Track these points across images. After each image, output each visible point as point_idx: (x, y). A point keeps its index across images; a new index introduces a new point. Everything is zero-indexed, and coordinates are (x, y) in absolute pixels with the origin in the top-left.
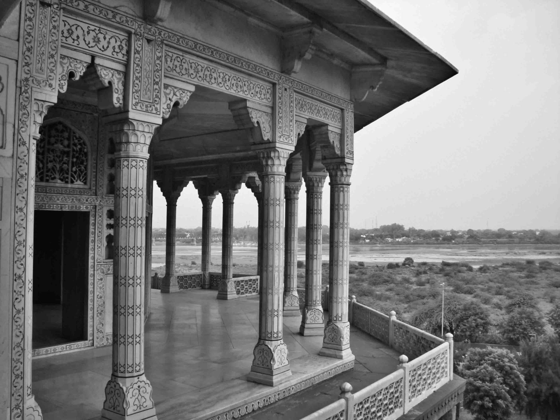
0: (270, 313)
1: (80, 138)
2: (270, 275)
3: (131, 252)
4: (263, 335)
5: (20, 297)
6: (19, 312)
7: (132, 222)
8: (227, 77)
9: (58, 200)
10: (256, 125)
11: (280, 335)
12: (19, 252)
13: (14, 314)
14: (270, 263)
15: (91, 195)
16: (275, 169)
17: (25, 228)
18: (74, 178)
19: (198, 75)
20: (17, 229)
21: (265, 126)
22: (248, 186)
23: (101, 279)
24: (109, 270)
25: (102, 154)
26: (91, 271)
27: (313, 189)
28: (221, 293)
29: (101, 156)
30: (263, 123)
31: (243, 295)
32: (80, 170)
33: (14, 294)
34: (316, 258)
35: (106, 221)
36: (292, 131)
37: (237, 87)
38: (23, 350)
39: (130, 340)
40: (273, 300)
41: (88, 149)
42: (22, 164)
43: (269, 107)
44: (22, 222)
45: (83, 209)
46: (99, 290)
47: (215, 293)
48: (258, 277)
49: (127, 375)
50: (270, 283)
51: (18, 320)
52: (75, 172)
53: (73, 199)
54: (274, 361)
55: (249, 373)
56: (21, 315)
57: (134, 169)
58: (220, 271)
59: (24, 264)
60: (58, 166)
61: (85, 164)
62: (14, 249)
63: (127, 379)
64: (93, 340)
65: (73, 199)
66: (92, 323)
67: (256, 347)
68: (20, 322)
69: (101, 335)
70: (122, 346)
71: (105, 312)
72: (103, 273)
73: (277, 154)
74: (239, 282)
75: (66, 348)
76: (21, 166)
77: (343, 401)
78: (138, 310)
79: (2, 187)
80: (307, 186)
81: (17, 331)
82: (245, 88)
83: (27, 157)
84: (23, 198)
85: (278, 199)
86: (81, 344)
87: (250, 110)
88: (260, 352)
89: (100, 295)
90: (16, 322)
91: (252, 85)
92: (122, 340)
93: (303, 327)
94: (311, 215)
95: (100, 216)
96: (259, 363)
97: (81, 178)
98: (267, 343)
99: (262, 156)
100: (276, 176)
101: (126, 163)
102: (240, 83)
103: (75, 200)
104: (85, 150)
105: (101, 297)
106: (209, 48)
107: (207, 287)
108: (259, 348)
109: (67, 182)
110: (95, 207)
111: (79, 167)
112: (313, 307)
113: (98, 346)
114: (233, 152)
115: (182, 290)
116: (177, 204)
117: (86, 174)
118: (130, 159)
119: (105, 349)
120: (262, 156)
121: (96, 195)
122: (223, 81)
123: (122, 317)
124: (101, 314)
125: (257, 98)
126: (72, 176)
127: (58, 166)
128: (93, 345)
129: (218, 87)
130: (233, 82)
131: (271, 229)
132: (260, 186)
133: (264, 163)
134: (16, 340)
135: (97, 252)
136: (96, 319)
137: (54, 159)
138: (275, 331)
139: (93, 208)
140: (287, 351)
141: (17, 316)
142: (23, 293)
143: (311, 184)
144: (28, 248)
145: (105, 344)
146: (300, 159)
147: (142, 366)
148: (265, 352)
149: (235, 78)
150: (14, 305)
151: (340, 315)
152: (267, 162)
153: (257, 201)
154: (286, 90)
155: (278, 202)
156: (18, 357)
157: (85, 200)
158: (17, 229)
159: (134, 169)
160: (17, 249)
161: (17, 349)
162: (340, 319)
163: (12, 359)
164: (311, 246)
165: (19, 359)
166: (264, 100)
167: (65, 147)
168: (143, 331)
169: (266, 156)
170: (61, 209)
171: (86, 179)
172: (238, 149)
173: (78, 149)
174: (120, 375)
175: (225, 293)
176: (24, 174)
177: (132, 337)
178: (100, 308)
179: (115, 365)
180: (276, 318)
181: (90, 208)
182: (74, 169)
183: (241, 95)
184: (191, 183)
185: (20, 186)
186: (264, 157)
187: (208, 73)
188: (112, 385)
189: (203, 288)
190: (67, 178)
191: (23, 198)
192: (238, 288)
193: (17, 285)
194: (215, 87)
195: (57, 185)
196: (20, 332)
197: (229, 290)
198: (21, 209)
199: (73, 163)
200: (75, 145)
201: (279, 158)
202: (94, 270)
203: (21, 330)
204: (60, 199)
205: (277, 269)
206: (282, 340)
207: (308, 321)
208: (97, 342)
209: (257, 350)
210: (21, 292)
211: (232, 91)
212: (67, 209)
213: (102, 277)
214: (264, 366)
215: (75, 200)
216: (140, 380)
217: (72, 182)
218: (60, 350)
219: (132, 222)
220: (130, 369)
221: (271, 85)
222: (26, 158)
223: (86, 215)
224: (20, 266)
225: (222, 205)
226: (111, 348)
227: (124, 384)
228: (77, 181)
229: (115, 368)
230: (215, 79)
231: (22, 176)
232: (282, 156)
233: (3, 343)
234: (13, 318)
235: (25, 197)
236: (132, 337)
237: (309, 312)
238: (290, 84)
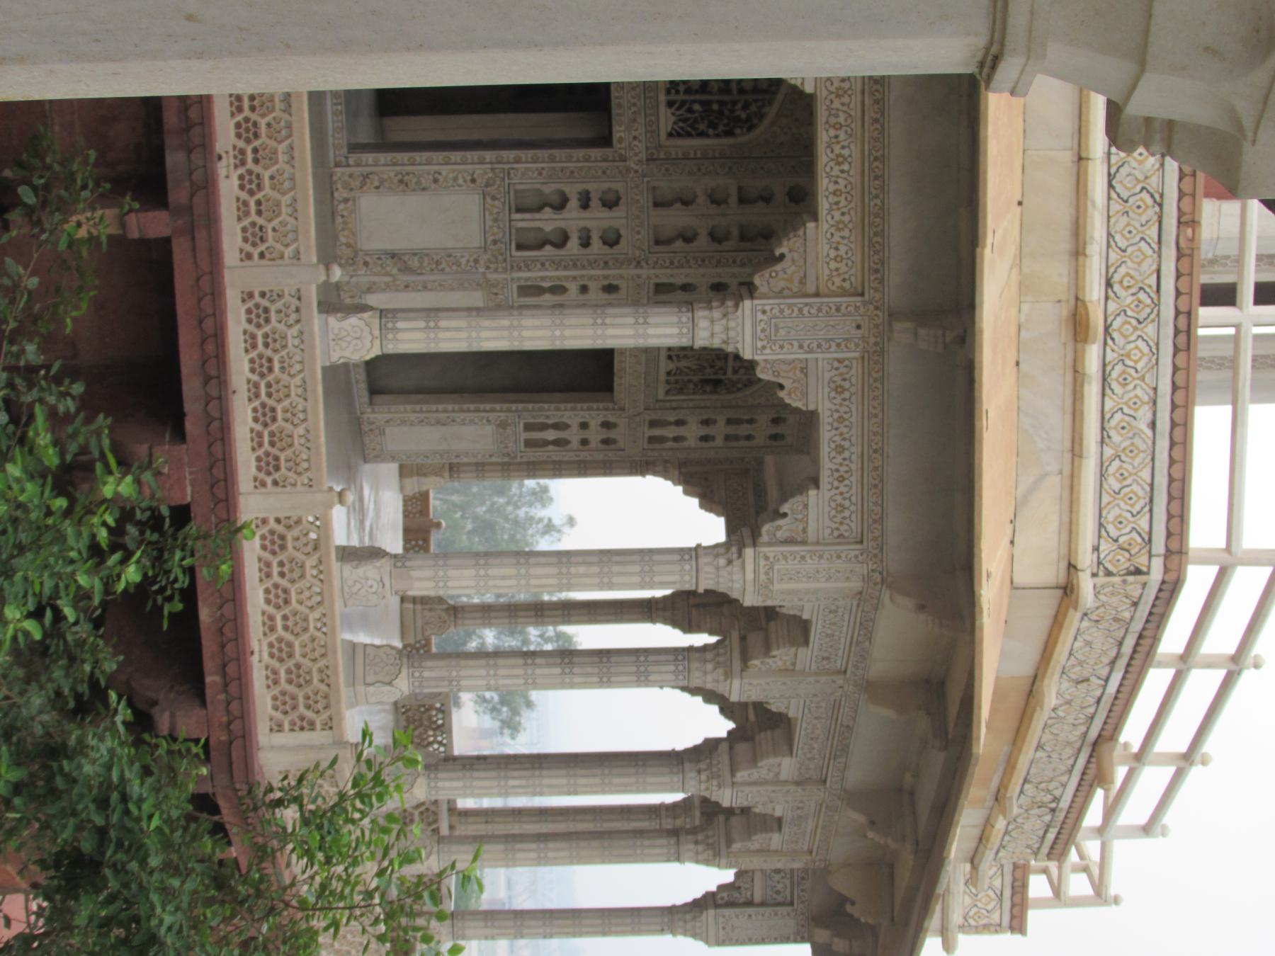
1: (761, 117)
8: (846, 167)
10: (777, 252)
15: (647, 148)
18: (678, 109)
19: (833, 96)
21: (781, 275)
23: (473, 181)
24: (494, 198)
29: (730, 168)
30: (784, 271)
32: (696, 120)
34: (526, 664)
36: (782, 347)
37: (834, 193)
41: (743, 138)
43: (818, 287)
45: (618, 131)
46: (451, 175)
52: (690, 111)
53: (634, 105)
61: (711, 131)
64: (348, 166)
69: (358, 184)
72: (487, 185)
73: (730, 310)
75: (336, 104)
77: (315, 260)
82: (837, 215)
87: (801, 233)
89: (441, 178)
91: (846, 233)
95: (604, 173)
97: (681, 124)
102: (842, 199)
103: (633, 109)
104: (738, 131)
105: (436, 181)
106: (883, 114)
110: (623, 159)
111: (703, 119)
112: (405, 660)
113: (335, 178)
117: (689, 135)
121: (648, 160)
122: (838, 156)
124: (401, 181)
125: (826, 247)
126: (683, 103)
128: (337, 165)
129: (824, 145)
130: (842, 182)
136: (389, 172)
145: (336, 195)
149: (849, 187)
151: (408, 564)
153: (689, 899)
154: (858, 327)
155: (641, 320)
162: (399, 564)
166: (827, 272)
171: (679, 135)
173: (738, 113)
178: (414, 180)
182: (697, 107)
183: (823, 205)
187: (842, 119)
190: (677, 92)
194: (823, 137)
199: (709, 103)
200: (746, 106)
201: (725, 315)
208: (343, 174)
211: (825, 181)
213: (478, 181)
215: (633, 109)
217: (670, 104)
221: (860, 290)
223: (604, 140)
230: (836, 137)
238: (872, 340)
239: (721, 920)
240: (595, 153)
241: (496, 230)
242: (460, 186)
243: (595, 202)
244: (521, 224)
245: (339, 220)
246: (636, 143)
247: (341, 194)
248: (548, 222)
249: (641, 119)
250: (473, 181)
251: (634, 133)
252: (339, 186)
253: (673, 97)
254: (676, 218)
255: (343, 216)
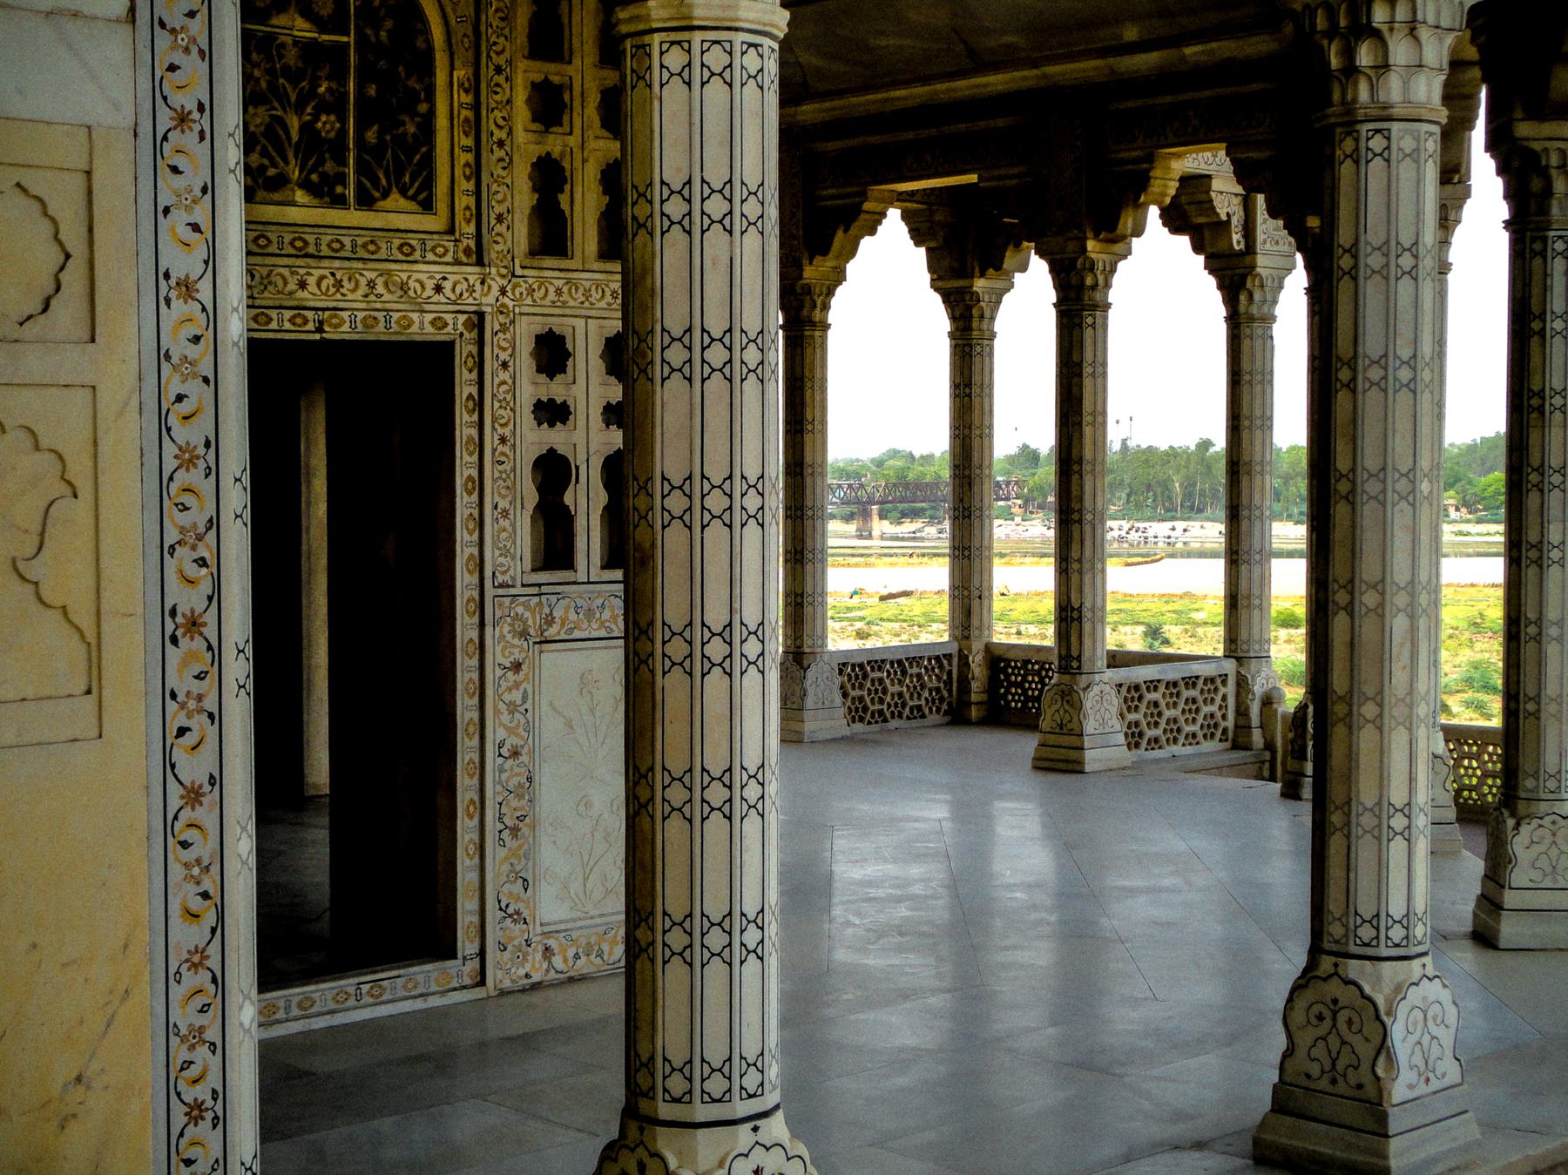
0: (1367, 820)
2: (1367, 629)
3: (716, 502)
4: (1336, 930)
5: (199, 723)
6: (194, 796)
7: (717, 355)
9: (303, 285)
11: (1419, 931)
12: (187, 499)
13: (174, 803)
14: (1368, 569)
15: (457, 262)
16: (1393, 89)
17: (212, 382)
20: (174, 387)
22: (1175, 220)
23: (517, 666)
24: (550, 620)
25: (501, 60)
26: (465, 628)
27: (1544, 211)
28: (1052, 739)
29: (499, 70)
31: (1157, 754)
33: (172, 706)
35: (530, 387)
38: (218, 981)
39: (716, 939)
40: (1382, 752)
42: (177, 58)
44: (193, 351)
45: (421, 328)
46: (505, 718)
47: (1025, 745)
48: (1230, 667)
49: (703, 1112)
50: (1366, 669)
51: (190, 835)
52: (378, 151)
53: (371, 284)
54: (1391, 1061)
55: (1263, 1125)
56: (205, 815)
57: (716, 88)
58: (1049, 642)
59: (212, 561)
60: (294, 123)
62: (164, 482)
63: (701, 1132)
64: (482, 954)
65: (371, 284)
66: (474, 876)
67: (1297, 988)
68: (204, 849)
70: (676, 969)
71: (533, 827)
72: (524, 634)
74: (1137, 688)
76: (172, 68)
78: (752, 792)
79: (89, 173)
80: (1513, 195)
81: (192, 889)
83: (201, 18)
84: (196, 228)
85: (1406, 241)
86: (426, 974)
88: (1320, 1018)
90: (185, 845)
92: (677, 939)
93: (1490, 903)
94: (1535, 341)
96: (1315, 1069)
98: (1353, 968)
99: (1321, 23)
100: (1396, 127)
101: (675, 59)
103: (380, 289)
105: (515, 754)
107: (974, 713)
108: (1309, 995)
109: (339, 202)
110: (478, 321)
112: (1543, 807)
113: (507, 984)
114: (1104, 53)
115: (859, 727)
116: (832, 317)
117: (428, 161)
118: (697, 37)
119: (536, 998)
120: (1321, 23)
121: (480, 262)
123: (675, 822)
124: (515, 831)
126: (362, 168)
127: (294, 123)
128: (482, 982)
131: (1371, 402)
132: (1237, 222)
133: (1335, 62)
134: (187, 936)
135: (492, 530)
137: (273, 86)
138: (1397, 908)
139: (469, 325)
140: (1452, 1012)
141: (186, 815)
142: (210, 704)
143: (1536, 184)
144: (227, 481)
145: (536, 978)
146: (1471, 64)
147: (773, 1071)
148: (1343, 1016)
150: (170, 766)
152: (1349, 54)
153: (1218, 296)
155: (1406, 261)
156: (200, 1020)
157: (430, 284)
158: (174, 387)
159: (716, 88)
160: (174, 487)
161: (191, 980)
163: (170, 1028)
164: (1533, 500)
165: (202, 1029)
167: (323, 29)
168: (773, 896)
169: (1343, 23)
170: (320, 330)
171: (429, 184)
172: (1131, 34)
174: (665, 1111)
175: (1073, 740)
176: (191, 105)
177: (725, 923)
178: (514, 803)
179: (640, 1067)
180: (1397, 847)
181: (456, 325)
182: (371, 136)
184: (894, 214)
185: (175, 170)
186: (1333, 32)
188: (629, 1162)
189: (957, 717)
191: (196, 228)
192: (1132, 717)
193: (185, 663)
195: (293, 214)
196: (205, 895)
197: (1090, 726)
198: (187, 288)
201: (1412, 32)
202: (482, 625)
203: (209, 885)
204: (312, 281)
205: (1401, 600)
206: (1427, 960)
207: (1518, 877)
209: (1301, 1004)
210: (200, 698)
212: (342, 331)
213: (518, 655)
214: (1341, 1088)
216: (762, 1136)
217: (366, 201)
218: (332, 1006)
219: (717, 355)
220: (716, 1085)
222: (197, 26)
224: (192, 571)
225: (1051, 316)
226: (620, 984)
227: (688, 1158)
228: (385, 195)
229: (643, 1080)
231: (183, 119)
232: (1431, 20)
233: (126, 947)
234: (168, 828)
235: (206, 226)
236: (725, 923)
237: (1525, 829)
239: (1268, 246)
240: (464, 386)
241: (607, 614)
242: (525, 699)
243: (556, 390)
244: (596, 559)
245: (583, 966)
246: (447, 285)
247: (536, 968)
248: (587, 501)
249: (401, 273)
250: (517, 666)
251: (429, 292)
252: (522, 972)
253: (351, 193)
254: (585, 205)
255: (577, 957)
